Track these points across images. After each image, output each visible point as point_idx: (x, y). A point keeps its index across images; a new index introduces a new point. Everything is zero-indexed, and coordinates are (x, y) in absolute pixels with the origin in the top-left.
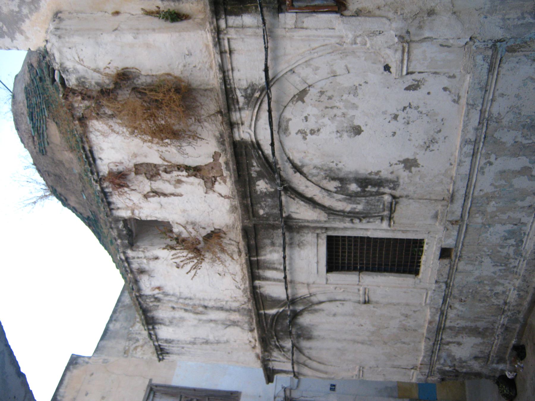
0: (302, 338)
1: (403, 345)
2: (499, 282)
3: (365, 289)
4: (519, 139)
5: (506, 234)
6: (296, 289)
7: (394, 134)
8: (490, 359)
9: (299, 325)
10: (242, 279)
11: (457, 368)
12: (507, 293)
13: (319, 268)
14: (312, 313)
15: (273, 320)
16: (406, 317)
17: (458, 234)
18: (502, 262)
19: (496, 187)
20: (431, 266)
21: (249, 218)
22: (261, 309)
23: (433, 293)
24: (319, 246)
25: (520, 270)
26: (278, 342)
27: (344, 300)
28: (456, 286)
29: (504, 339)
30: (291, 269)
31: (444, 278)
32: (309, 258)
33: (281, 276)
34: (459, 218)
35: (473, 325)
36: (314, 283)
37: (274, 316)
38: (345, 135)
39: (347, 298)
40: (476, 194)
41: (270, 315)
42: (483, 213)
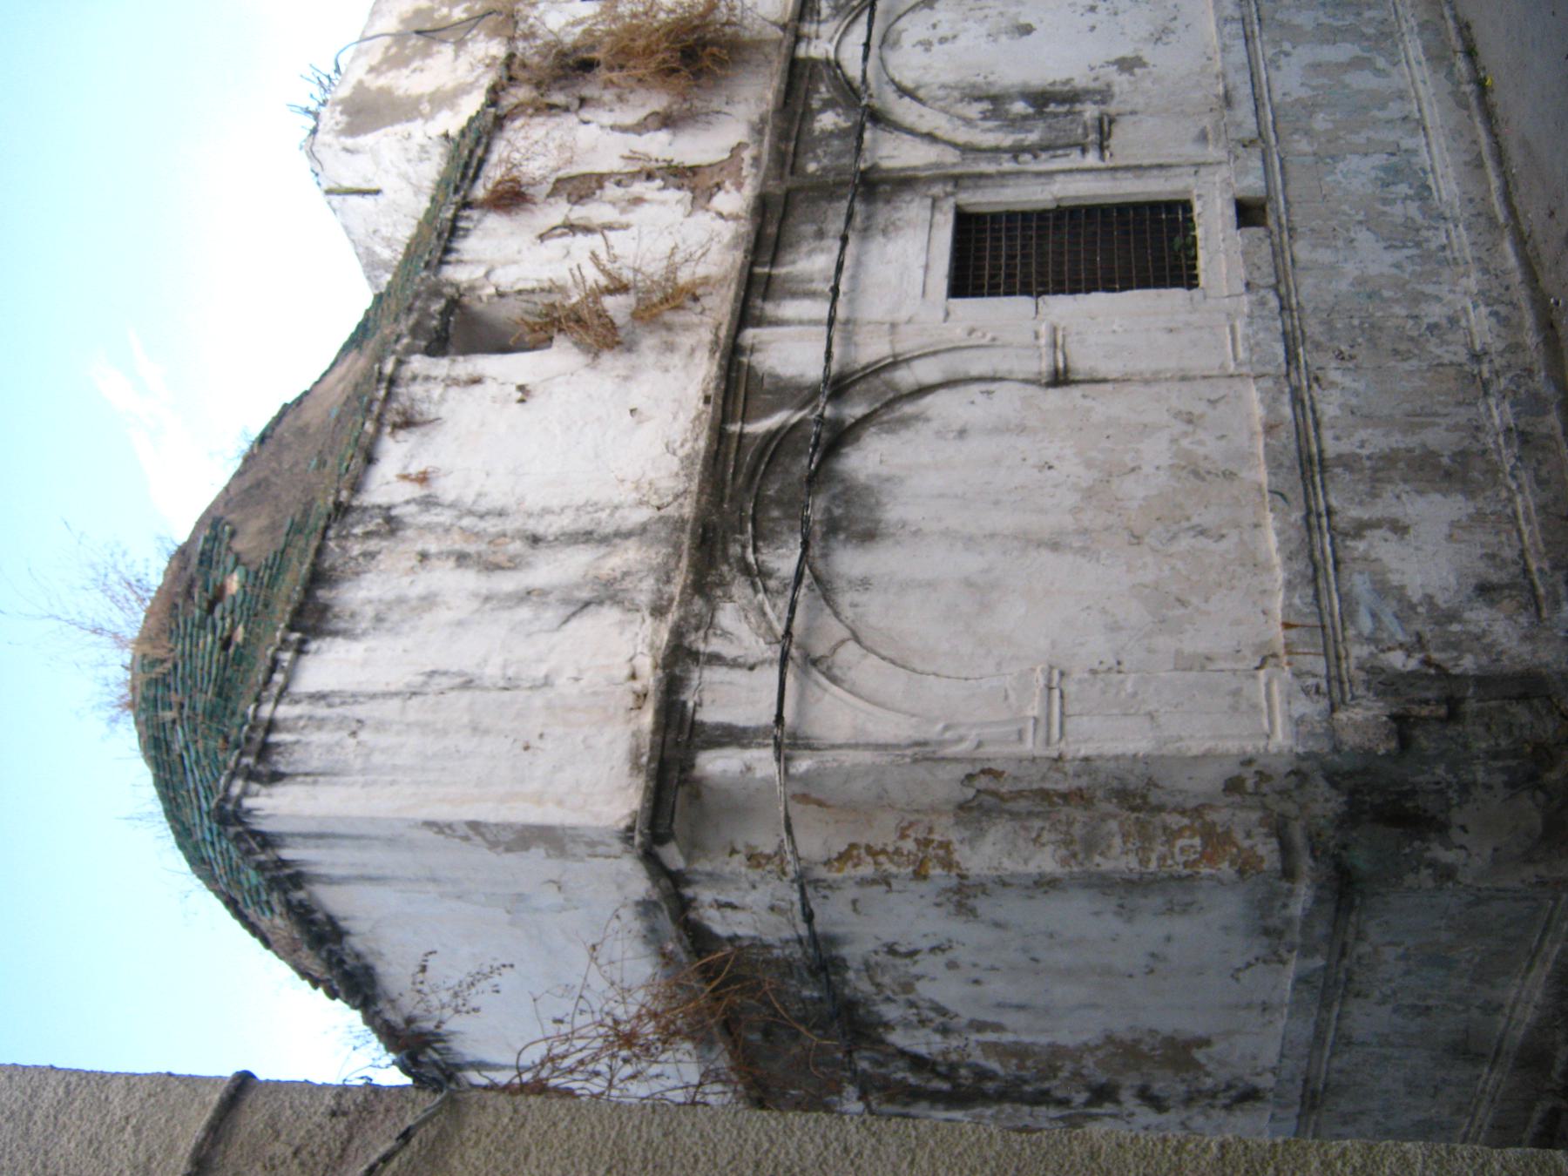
0: (842, 536)
1: (1202, 542)
2: (1423, 293)
3: (1054, 330)
4: (1323, 19)
5: (1382, 175)
6: (856, 345)
7: (1093, 28)
8: (1541, 591)
9: (843, 481)
10: (693, 421)
11: (1436, 656)
12: (1463, 323)
13: (929, 282)
14: (891, 431)
15: (761, 453)
16: (1190, 422)
17: (1264, 161)
18: (1402, 236)
19: (1314, 88)
20: (1223, 246)
21: (781, 177)
22: (734, 421)
23: (1250, 324)
24: (934, 231)
25: (1461, 250)
26: (756, 550)
27: (994, 379)
28: (1309, 307)
29: (1541, 483)
30: (853, 290)
31: (1266, 276)
32: (905, 262)
33: (820, 309)
34: (1255, 135)
35: (1412, 441)
36: (909, 321)
37: (771, 435)
38: (1003, 39)
39: (1002, 367)
40: (1277, 98)
41: (755, 436)
42: (1308, 133)
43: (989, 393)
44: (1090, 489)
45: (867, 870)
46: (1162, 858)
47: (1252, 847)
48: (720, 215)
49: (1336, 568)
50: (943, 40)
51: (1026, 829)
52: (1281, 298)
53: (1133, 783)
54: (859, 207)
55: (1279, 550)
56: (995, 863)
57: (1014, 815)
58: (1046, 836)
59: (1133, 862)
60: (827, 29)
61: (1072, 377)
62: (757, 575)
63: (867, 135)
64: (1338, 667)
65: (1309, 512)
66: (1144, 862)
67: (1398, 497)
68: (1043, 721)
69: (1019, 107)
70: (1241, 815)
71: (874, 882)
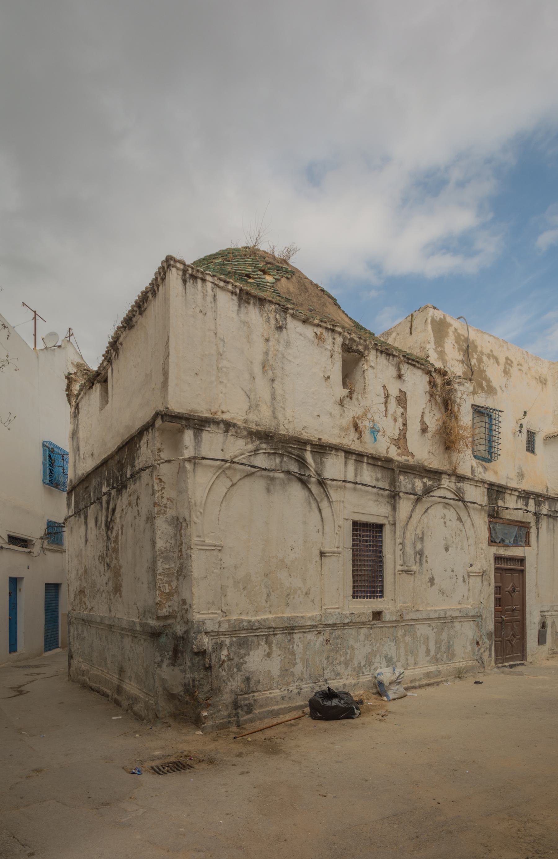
1: (265, 596)
5: (389, 657)
7: (446, 571)
12: (338, 678)
38: (444, 542)
43: (319, 531)
44: (284, 561)
45: (156, 488)
46: (161, 580)
47: (165, 607)
48: (388, 448)
49: (255, 636)
50: (445, 523)
51: (171, 538)
52: (347, 623)
53: (185, 571)
54: (387, 493)
55: (262, 619)
56: (159, 528)
57: (175, 535)
58: (168, 544)
59: (160, 571)
60: (452, 485)
61: (323, 558)
62: (255, 452)
63: (412, 496)
64: (222, 635)
65: (275, 628)
66: (160, 574)
67: (279, 655)
68: (204, 543)
69: (419, 546)
70: (176, 604)
71: (153, 490)
